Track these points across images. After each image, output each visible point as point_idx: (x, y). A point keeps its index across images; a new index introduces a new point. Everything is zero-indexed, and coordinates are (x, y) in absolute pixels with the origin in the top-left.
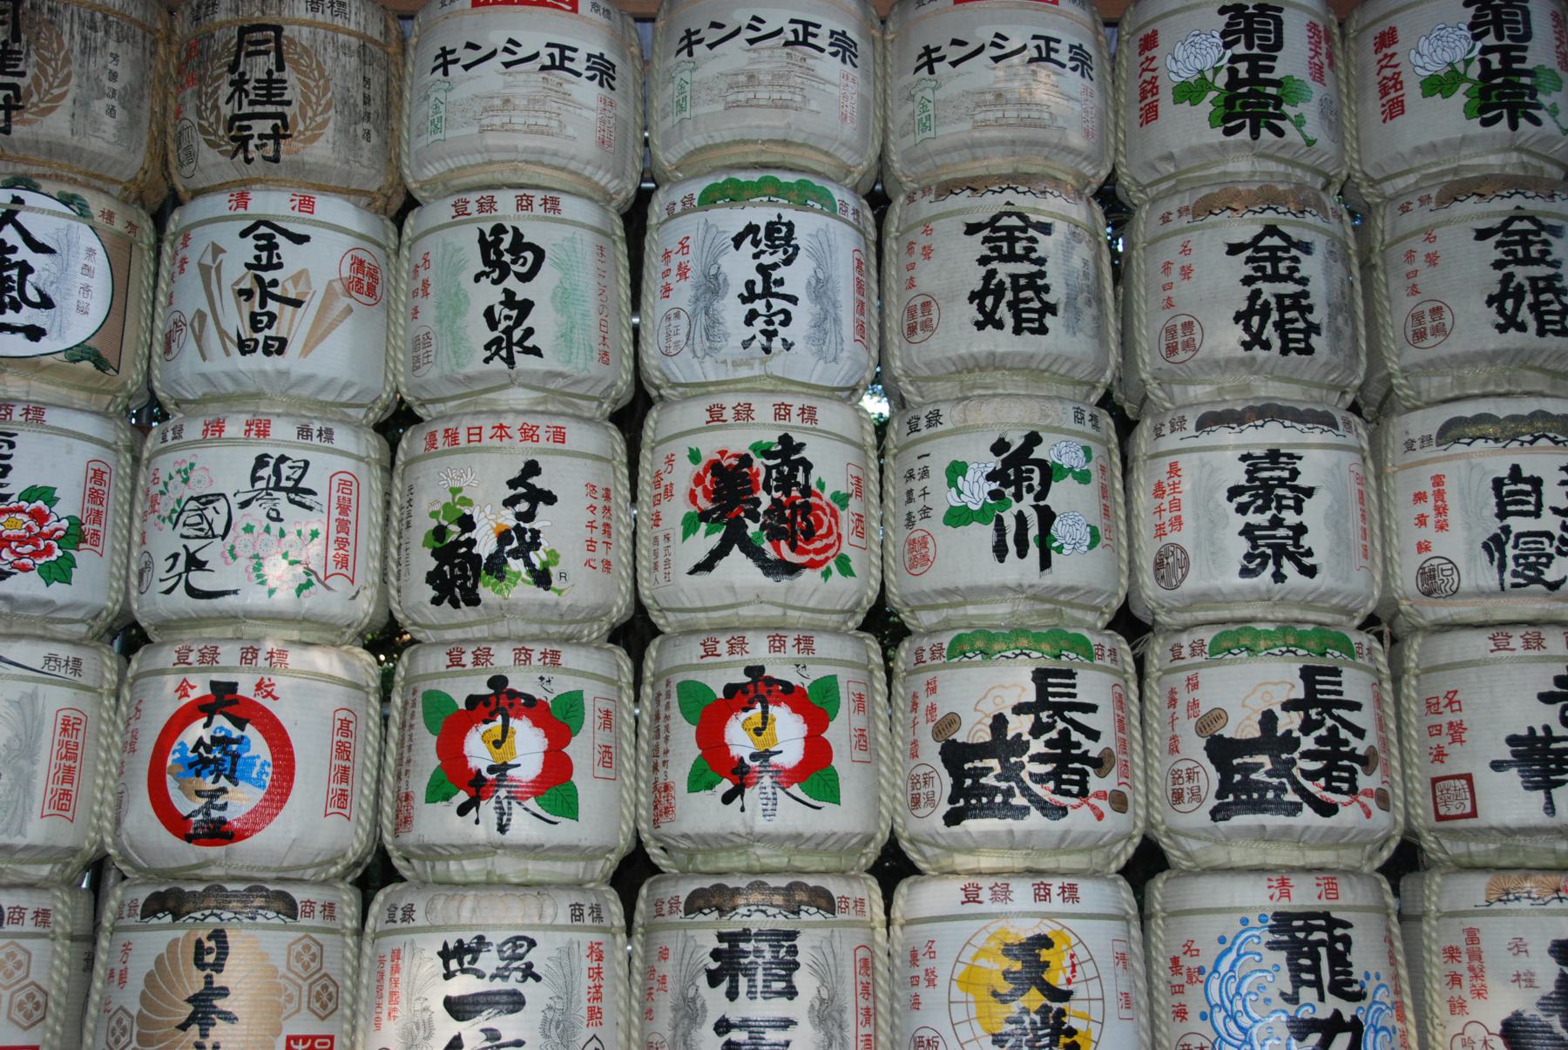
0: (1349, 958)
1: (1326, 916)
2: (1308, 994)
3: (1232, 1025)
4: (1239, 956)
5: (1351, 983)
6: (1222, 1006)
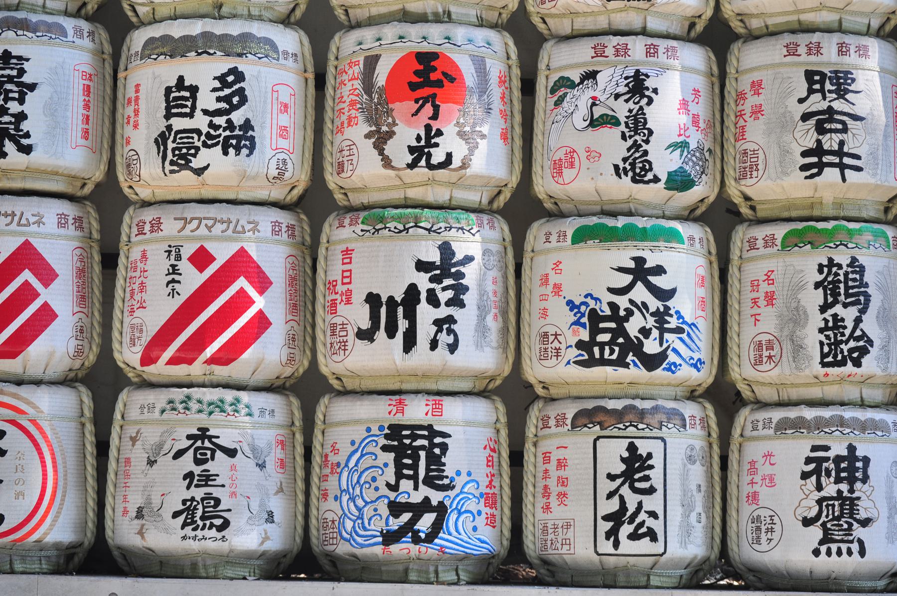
0: (443, 460)
1: (429, 428)
2: (406, 485)
3: (352, 505)
4: (362, 456)
5: (442, 478)
6: (347, 491)
